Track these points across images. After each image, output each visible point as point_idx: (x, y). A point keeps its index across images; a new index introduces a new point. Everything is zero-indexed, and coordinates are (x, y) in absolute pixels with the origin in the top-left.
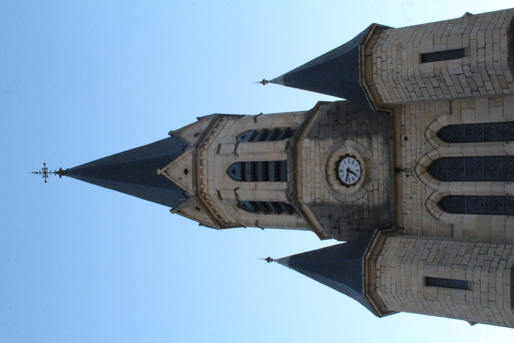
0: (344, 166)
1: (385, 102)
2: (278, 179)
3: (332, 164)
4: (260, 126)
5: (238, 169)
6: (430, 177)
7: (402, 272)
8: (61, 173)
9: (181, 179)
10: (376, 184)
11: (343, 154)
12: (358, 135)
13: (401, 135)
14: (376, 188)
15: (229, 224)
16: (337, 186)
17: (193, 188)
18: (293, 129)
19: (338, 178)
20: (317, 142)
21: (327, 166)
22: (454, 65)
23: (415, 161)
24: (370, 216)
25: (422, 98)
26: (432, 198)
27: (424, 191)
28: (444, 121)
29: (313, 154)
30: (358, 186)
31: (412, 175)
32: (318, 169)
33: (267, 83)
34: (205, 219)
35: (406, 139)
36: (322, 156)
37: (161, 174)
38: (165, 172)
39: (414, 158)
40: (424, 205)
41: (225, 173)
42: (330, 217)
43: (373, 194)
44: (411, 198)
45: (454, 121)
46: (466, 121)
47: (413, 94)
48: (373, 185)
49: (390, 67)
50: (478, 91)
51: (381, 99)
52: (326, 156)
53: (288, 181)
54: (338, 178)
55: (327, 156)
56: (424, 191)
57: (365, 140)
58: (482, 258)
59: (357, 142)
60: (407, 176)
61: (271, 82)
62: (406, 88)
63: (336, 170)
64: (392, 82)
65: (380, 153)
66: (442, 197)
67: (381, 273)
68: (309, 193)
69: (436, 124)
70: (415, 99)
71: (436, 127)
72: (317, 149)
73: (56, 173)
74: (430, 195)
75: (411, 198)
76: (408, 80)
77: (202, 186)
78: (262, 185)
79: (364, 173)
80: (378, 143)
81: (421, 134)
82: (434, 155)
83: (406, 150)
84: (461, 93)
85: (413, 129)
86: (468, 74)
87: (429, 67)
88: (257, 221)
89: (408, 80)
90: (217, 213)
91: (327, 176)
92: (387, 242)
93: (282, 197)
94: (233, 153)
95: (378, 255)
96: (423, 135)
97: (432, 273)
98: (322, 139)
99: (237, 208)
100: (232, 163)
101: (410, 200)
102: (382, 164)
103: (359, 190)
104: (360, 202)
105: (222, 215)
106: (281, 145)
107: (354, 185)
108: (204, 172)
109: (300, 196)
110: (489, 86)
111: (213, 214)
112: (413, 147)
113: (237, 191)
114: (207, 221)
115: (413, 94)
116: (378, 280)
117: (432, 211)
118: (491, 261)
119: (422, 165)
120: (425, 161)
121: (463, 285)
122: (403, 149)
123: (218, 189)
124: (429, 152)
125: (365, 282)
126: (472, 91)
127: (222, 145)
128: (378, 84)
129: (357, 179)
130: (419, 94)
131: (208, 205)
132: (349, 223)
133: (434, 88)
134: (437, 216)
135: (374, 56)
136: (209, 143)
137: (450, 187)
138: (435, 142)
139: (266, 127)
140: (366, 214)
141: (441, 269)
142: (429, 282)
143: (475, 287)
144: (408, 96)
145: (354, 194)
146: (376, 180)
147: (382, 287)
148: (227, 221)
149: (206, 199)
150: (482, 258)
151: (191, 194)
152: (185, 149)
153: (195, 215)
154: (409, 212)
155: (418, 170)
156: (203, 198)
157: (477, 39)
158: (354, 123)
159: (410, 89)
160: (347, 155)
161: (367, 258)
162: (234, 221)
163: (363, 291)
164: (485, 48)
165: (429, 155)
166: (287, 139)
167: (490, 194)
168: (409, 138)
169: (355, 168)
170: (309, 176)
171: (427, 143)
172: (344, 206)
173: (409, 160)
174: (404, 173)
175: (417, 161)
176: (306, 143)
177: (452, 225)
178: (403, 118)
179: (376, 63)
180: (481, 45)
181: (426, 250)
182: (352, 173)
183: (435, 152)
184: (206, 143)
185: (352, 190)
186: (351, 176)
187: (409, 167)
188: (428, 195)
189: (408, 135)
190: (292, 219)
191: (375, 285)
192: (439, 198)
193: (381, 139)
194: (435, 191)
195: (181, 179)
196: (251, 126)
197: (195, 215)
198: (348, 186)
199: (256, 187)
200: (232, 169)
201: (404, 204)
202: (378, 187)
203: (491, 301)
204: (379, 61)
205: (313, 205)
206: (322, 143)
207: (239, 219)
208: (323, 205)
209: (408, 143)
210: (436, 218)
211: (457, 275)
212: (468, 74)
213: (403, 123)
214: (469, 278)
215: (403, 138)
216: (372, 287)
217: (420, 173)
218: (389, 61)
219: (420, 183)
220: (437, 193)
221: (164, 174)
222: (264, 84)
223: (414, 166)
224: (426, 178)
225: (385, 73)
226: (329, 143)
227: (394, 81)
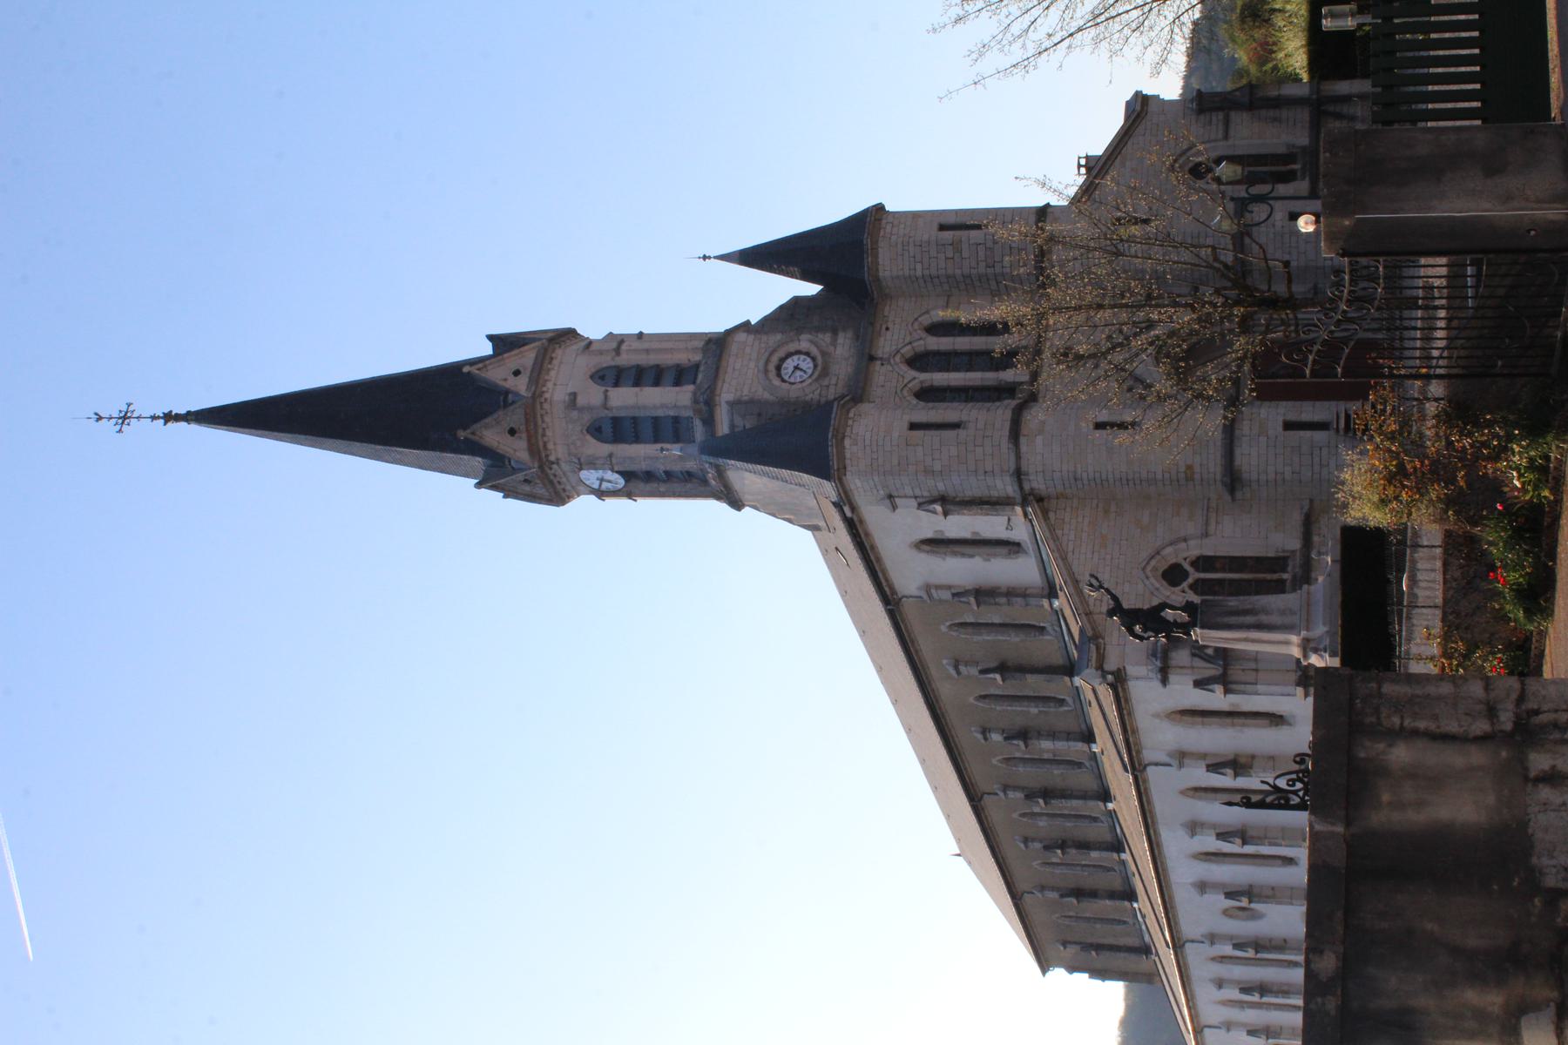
0: (790, 364)
3: (775, 359)
8: (169, 417)
11: (792, 350)
12: (818, 329)
13: (881, 326)
14: (833, 382)
16: (777, 382)
20: (759, 336)
21: (767, 362)
26: (910, 385)
31: (889, 363)
32: (752, 365)
34: (515, 450)
35: (887, 329)
37: (469, 373)
39: (894, 347)
42: (759, 415)
43: (828, 389)
44: (883, 386)
47: (919, 266)
48: (830, 379)
51: (877, 270)
53: (698, 381)
60: (882, 364)
61: (715, 257)
64: (900, 246)
66: (922, 388)
67: (853, 421)
68: (733, 391)
69: (927, 316)
71: (926, 320)
73: (154, 418)
74: (910, 382)
75: (883, 386)
76: (921, 246)
79: (819, 368)
83: (885, 340)
86: (990, 244)
87: (948, 235)
88: (611, 456)
89: (921, 246)
90: (545, 439)
91: (766, 371)
94: (614, 350)
96: (910, 326)
98: (766, 333)
99: (585, 432)
100: (605, 365)
104: (808, 398)
108: (553, 373)
109: (718, 392)
111: (540, 438)
112: (895, 337)
114: (518, 454)
115: (919, 266)
116: (849, 429)
119: (903, 355)
122: (882, 339)
125: (834, 425)
126: (987, 266)
129: (805, 376)
131: (540, 422)
133: (946, 258)
135: (884, 222)
138: (924, 335)
142: (913, 426)
147: (852, 436)
149: (542, 408)
151: (525, 395)
153: (499, 443)
155: (898, 358)
160: (798, 352)
165: (915, 344)
168: (891, 329)
169: (807, 364)
170: (737, 373)
173: (887, 349)
174: (879, 362)
178: (887, 308)
179: (885, 228)
182: (801, 370)
183: (922, 342)
186: (798, 373)
187: (885, 356)
188: (906, 381)
189: (890, 325)
191: (844, 433)
192: (917, 388)
193: (850, 334)
194: (914, 378)
197: (499, 443)
200: (601, 374)
202: (837, 381)
203: (987, 437)
206: (764, 338)
208: (751, 402)
209: (889, 333)
212: (990, 244)
213: (886, 314)
214: (964, 418)
215: (884, 327)
216: (840, 436)
218: (902, 226)
220: (916, 381)
224: (904, 368)
225: (894, 238)
226: (779, 337)
227: (903, 246)
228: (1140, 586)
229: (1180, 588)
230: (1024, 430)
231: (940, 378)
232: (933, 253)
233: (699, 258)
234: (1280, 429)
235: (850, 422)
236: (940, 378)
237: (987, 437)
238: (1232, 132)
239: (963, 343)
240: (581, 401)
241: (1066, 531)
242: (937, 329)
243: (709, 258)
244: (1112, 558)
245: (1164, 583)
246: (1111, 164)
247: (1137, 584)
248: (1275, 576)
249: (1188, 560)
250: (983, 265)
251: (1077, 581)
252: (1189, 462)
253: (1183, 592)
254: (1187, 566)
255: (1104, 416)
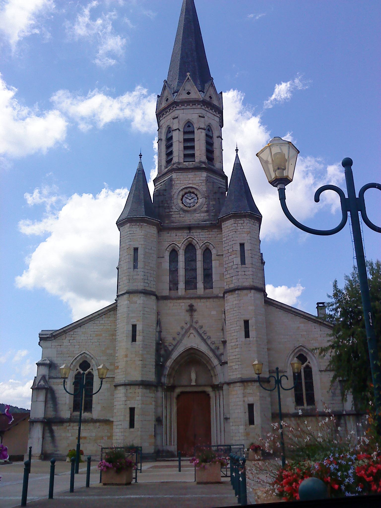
1: (223, 224)
2: (185, 156)
4: (216, 141)
5: (190, 129)
6: (186, 245)
7: (140, 237)
9: (184, 90)
10: (183, 216)
15: (159, 120)
16: (181, 193)
17: (179, 99)
18: (213, 161)
19: (186, 193)
20: (205, 181)
21: (192, 188)
22: (238, 260)
23: (194, 237)
24: (167, 213)
25: (224, 243)
26: (176, 246)
27: (180, 242)
28: (214, 252)
29: (198, 178)
30: (182, 206)
33: (236, 152)
36: (197, 184)
38: (188, 78)
40: (173, 242)
41: (188, 121)
42: (165, 190)
44: (176, 235)
45: (213, 257)
46: (213, 262)
47: (225, 239)
49: (239, 228)
50: (226, 271)
52: (197, 186)
53: (184, 163)
54: (186, 193)
55: (197, 187)
56: (180, 242)
57: (206, 209)
58: (149, 275)
59: (204, 205)
62: (228, 236)
63: (190, 192)
65: (199, 218)
70: (224, 239)
71: (211, 247)
72: (202, 181)
75: (176, 235)
77: (180, 106)
78: (182, 146)
80: (204, 216)
81: (207, 240)
82: (197, 247)
84: (225, 263)
85: (210, 236)
92: (154, 226)
93: (175, 160)
95: (147, 223)
96: (207, 241)
97: (140, 252)
101: (175, 235)
102: (193, 219)
103: (179, 207)
104: (174, 207)
105: (164, 116)
106: (204, 159)
107: (183, 203)
108: (189, 107)
110: (228, 276)
113: (178, 130)
115: (225, 239)
116: (135, 224)
117: (170, 247)
118: (148, 279)
120: (194, 242)
121: (135, 267)
123: (178, 117)
124: (199, 245)
127: (204, 118)
128: (231, 221)
130: (226, 242)
132: (162, 201)
134: (168, 249)
135: (245, 219)
136: (205, 108)
137: (182, 255)
139: (214, 144)
140: (168, 210)
141: (142, 256)
142: (136, 250)
143: (135, 273)
144: (225, 236)
145: (177, 204)
146: (185, 216)
148: (161, 119)
149: (173, 107)
150: (149, 275)
152: (201, 92)
154: (169, 235)
156: (173, 106)
157: (249, 271)
158: (214, 203)
159: (228, 238)
161: (145, 218)
162: (161, 123)
163: (129, 217)
164: (245, 275)
166: (206, 161)
167: (179, 274)
171: (203, 243)
172: (171, 198)
174: (188, 232)
175: (195, 239)
176: (204, 174)
177: (164, 257)
180: (246, 273)
181: (151, 247)
183: (199, 248)
184: (205, 106)
185: (180, 202)
188: (177, 244)
190: (164, 163)
195: (184, 90)
196: (216, 134)
198: (182, 200)
199: (180, 142)
201: (173, 232)
203: (129, 280)
204: (242, 222)
205: (171, 180)
206: (204, 184)
207: (162, 127)
210: (167, 249)
211: (140, 264)
217: (189, 240)
218: (242, 227)
219: (184, 240)
220: (179, 249)
221: (187, 78)
222: (236, 150)
223: (192, 237)
228: (77, 352)
229: (79, 368)
230: (132, 295)
231: (181, 258)
232: (230, 244)
233: (237, 148)
234: (130, 406)
235: (138, 224)
236: (181, 258)
237: (129, 280)
238: (323, 373)
239: (199, 265)
240: (176, 120)
241: (104, 319)
242: (207, 253)
243: (237, 152)
244: (91, 339)
245: (81, 362)
246: (301, 317)
247: (79, 350)
248: (83, 408)
249: (91, 370)
250: (226, 266)
251: (81, 326)
252: (119, 367)
253: (77, 370)
254: (88, 370)
255: (139, 328)
